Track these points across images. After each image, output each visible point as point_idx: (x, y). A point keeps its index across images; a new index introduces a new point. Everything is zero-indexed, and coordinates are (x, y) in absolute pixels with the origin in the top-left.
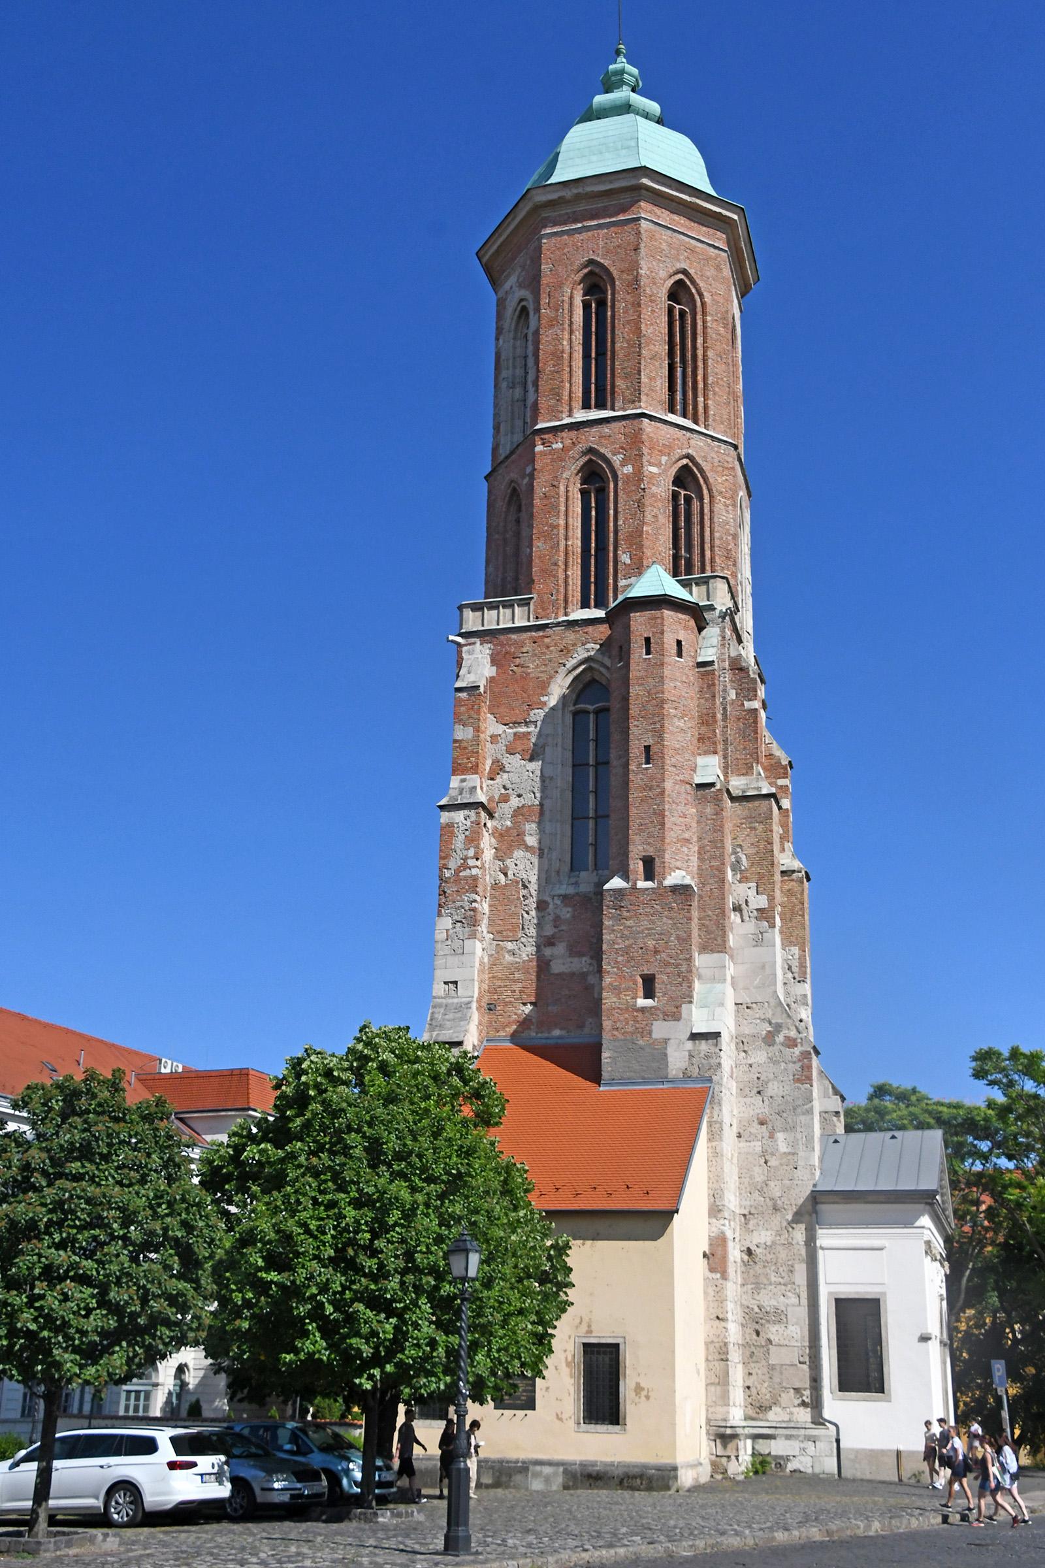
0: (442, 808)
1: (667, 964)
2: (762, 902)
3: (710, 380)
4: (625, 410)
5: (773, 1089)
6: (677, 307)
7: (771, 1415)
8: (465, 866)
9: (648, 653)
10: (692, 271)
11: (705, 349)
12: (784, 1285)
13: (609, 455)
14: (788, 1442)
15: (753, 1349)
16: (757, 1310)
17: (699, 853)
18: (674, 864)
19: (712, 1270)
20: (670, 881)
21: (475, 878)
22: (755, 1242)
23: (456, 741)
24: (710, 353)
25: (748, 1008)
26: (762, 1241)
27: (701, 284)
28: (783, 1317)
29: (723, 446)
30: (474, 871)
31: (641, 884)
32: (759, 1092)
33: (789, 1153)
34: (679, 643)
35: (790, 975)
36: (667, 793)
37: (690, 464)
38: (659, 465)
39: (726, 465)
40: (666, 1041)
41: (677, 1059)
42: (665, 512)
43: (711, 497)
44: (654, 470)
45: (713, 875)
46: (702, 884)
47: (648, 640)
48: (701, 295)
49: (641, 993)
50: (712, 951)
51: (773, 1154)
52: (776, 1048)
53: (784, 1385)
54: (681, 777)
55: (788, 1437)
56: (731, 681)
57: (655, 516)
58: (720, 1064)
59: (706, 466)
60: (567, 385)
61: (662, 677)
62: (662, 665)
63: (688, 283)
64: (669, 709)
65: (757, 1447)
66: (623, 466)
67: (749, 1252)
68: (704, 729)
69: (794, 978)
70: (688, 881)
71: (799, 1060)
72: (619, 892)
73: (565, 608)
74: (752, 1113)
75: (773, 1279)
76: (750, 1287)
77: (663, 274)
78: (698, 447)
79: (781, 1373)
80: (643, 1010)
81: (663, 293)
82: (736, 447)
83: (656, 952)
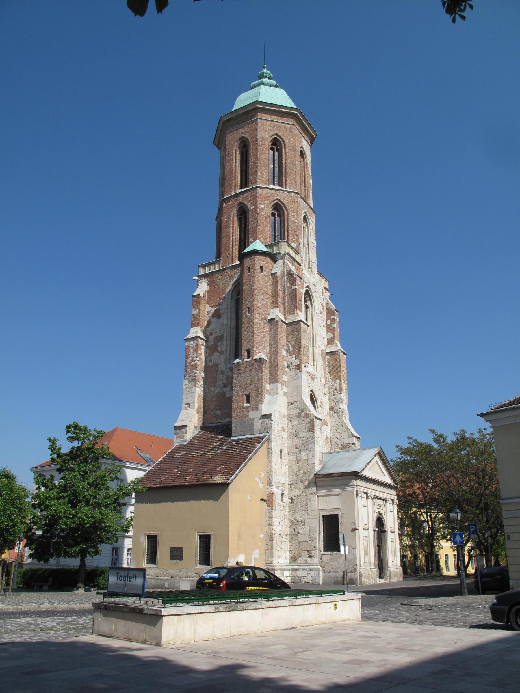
0: (186, 340)
1: (254, 389)
2: (297, 362)
3: (287, 171)
4: (252, 186)
5: (301, 435)
6: (275, 147)
7: (299, 561)
8: (193, 360)
9: (249, 273)
10: (279, 134)
11: (285, 160)
12: (304, 511)
13: (246, 204)
14: (303, 571)
15: (293, 536)
16: (294, 521)
17: (269, 346)
18: (257, 351)
19: (268, 506)
20: (255, 357)
21: (196, 364)
22: (294, 495)
23: (192, 315)
24: (287, 162)
25: (292, 404)
26: (296, 494)
27: (284, 138)
28: (303, 523)
29: (293, 194)
30: (196, 362)
31: (246, 360)
32: (296, 437)
33: (306, 459)
34: (261, 267)
35: (336, 391)
36: (255, 324)
37: (279, 202)
38: (264, 204)
39: (294, 200)
40: (253, 419)
41: (257, 424)
42: (267, 221)
43: (288, 213)
45: (274, 353)
46: (270, 358)
47: (249, 268)
48: (284, 141)
49: (245, 401)
50: (274, 383)
51: (300, 460)
52: (302, 418)
53: (304, 549)
54: (262, 317)
55: (303, 569)
56: (287, 279)
57: (263, 223)
58: (271, 426)
60: (234, 181)
61: (254, 281)
62: (254, 276)
63: (278, 138)
64: (257, 292)
65: (292, 573)
66: (251, 206)
67: (292, 499)
68: (274, 299)
69: (337, 392)
70: (263, 356)
71: (310, 423)
72: (238, 364)
73: (232, 261)
74: (293, 444)
75: (300, 509)
76: (292, 512)
77: (267, 136)
78: (281, 196)
79: (303, 545)
80: (246, 407)
81: (268, 144)
82: (298, 194)
83: (251, 385)
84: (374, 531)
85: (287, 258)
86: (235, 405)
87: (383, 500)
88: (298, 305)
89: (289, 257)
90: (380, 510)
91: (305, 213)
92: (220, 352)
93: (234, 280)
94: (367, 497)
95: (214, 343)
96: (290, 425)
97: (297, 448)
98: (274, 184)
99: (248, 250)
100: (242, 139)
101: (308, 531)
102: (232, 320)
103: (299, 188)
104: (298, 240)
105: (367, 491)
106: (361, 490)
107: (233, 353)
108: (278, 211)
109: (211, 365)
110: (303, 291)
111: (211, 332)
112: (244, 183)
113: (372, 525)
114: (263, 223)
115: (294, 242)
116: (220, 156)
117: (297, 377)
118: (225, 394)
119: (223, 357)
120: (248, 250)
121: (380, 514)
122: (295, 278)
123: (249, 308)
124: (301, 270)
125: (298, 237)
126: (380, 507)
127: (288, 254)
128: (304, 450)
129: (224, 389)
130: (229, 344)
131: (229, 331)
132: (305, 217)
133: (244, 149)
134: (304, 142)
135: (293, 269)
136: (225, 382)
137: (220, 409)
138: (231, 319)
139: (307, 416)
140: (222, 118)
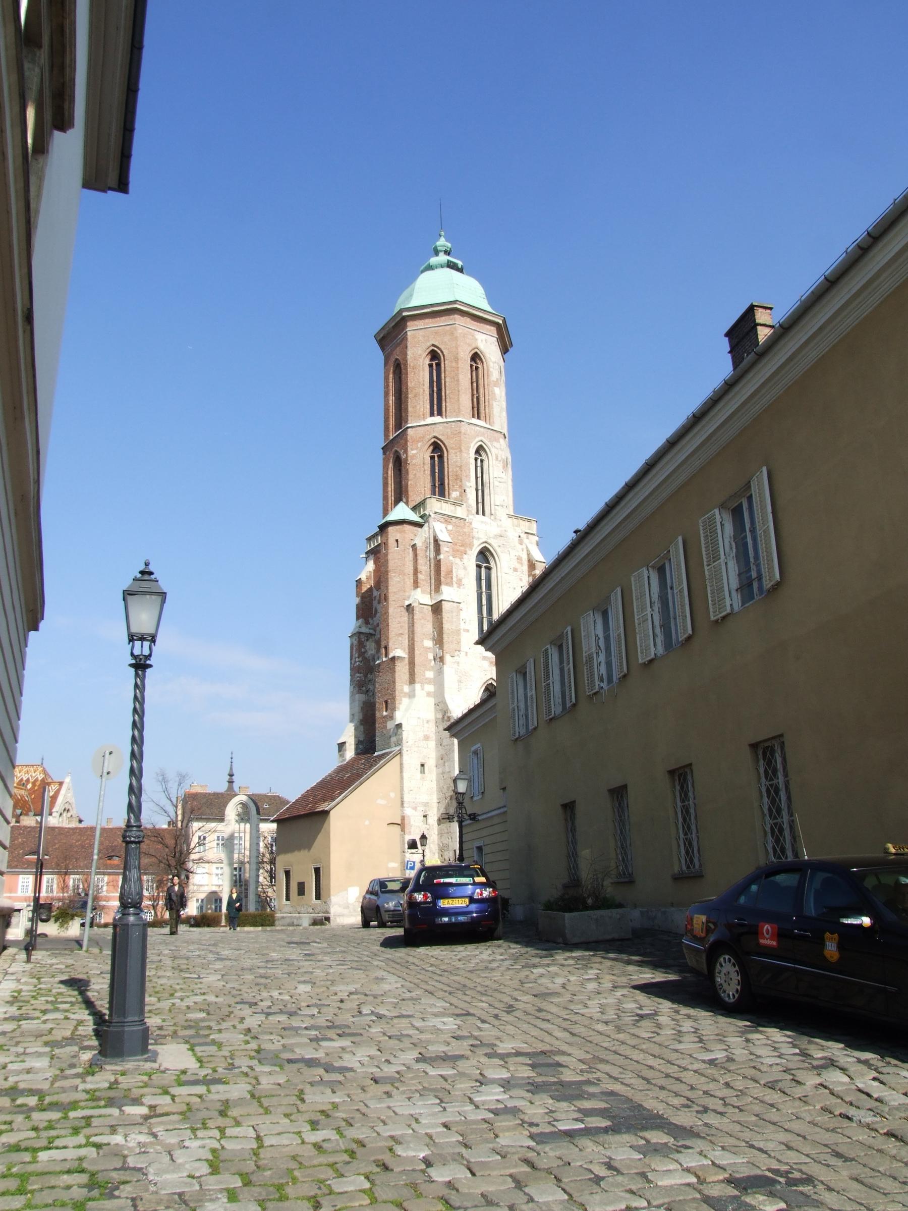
20: (390, 656)
44: (414, 452)
54: (398, 605)
72: (379, 664)
86: (378, 714)
114: (415, 475)
117: (440, 672)
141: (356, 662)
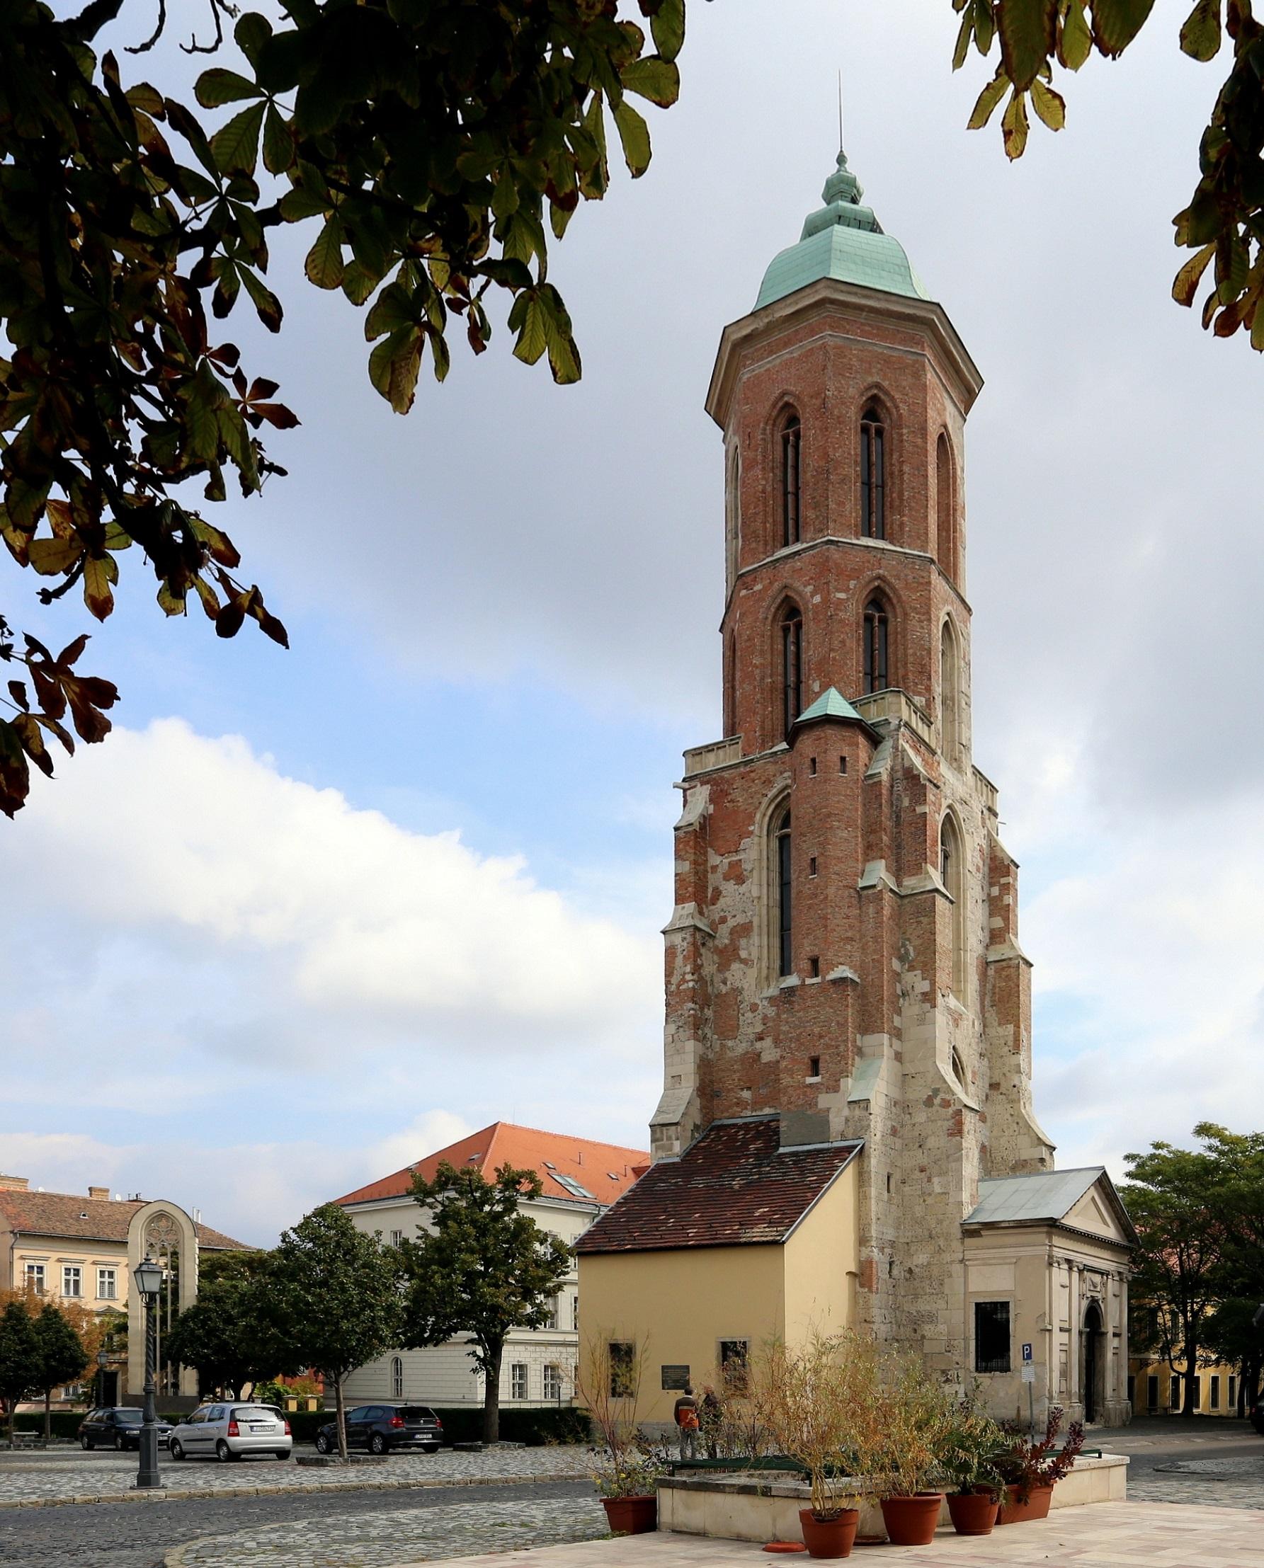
6: (874, 424)
10: (886, 384)
13: (801, 588)
37: (882, 585)
39: (921, 580)
48: (897, 407)
59: (898, 585)
81: (853, 415)
84: (1080, 1333)
85: (904, 735)
87: (1102, 1274)
88: (928, 853)
89: (907, 733)
90: (1094, 1294)
91: (948, 614)
92: (745, 962)
93: (775, 791)
94: (1070, 1269)
95: (732, 940)
96: (909, 1122)
97: (922, 1171)
98: (870, 536)
99: (806, 715)
100: (786, 399)
101: (945, 1332)
102: (771, 888)
103: (933, 545)
104: (929, 689)
105: (1072, 1255)
106: (1059, 1253)
107: (777, 965)
108: (881, 609)
109: (724, 992)
110: (940, 818)
111: (722, 914)
112: (791, 530)
113: (1077, 1323)
115: (920, 694)
116: (724, 447)
118: (759, 1055)
119: (752, 973)
120: (806, 715)
121: (1094, 1301)
122: (924, 786)
123: (813, 860)
124: (936, 764)
125: (929, 679)
126: (1095, 1287)
127: (907, 725)
128: (940, 1175)
129: (758, 1045)
130: (766, 943)
131: (764, 911)
132: (946, 624)
133: (790, 431)
134: (950, 408)
135: (917, 761)
136: (759, 1029)
137: (749, 1088)
138: (768, 885)
139: (946, 1104)
140: (728, 330)
141: (684, 981)
